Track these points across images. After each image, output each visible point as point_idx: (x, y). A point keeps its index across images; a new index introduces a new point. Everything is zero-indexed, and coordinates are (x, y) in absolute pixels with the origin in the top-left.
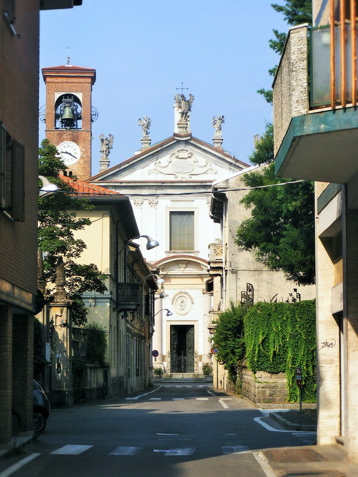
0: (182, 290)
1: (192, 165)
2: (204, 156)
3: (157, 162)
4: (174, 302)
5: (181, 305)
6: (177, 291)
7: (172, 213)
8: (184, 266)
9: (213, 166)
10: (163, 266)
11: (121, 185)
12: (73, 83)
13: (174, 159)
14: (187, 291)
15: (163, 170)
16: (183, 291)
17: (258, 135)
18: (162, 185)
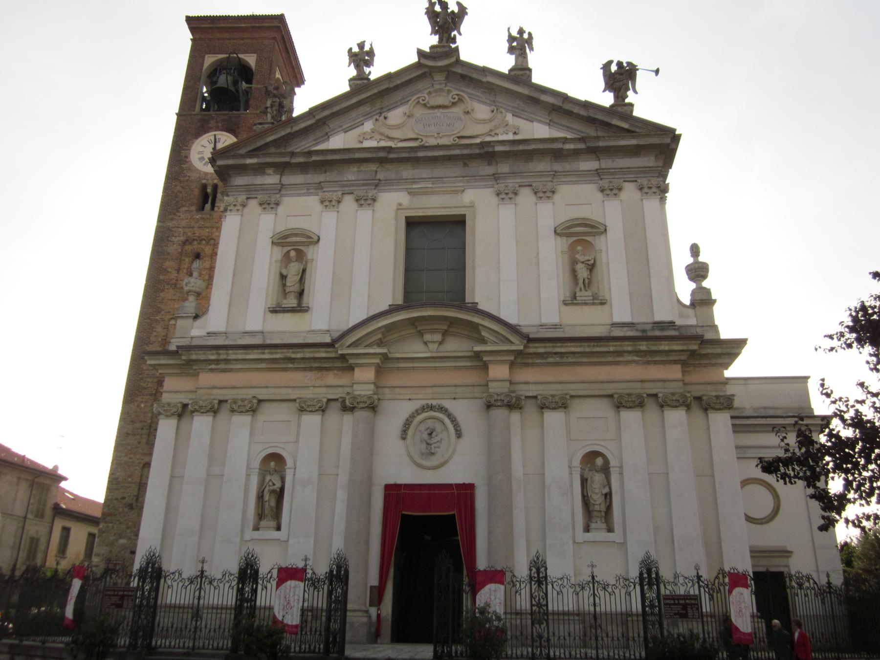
0: (430, 402)
1: (460, 119)
2: (488, 101)
3: (382, 118)
4: (410, 432)
5: (429, 441)
6: (417, 404)
7: (412, 224)
8: (438, 337)
9: (509, 117)
10: (380, 336)
11: (294, 161)
12: (243, 39)
13: (420, 112)
14: (447, 404)
15: (395, 134)
16: (434, 402)
17: (611, 62)
18: (384, 158)
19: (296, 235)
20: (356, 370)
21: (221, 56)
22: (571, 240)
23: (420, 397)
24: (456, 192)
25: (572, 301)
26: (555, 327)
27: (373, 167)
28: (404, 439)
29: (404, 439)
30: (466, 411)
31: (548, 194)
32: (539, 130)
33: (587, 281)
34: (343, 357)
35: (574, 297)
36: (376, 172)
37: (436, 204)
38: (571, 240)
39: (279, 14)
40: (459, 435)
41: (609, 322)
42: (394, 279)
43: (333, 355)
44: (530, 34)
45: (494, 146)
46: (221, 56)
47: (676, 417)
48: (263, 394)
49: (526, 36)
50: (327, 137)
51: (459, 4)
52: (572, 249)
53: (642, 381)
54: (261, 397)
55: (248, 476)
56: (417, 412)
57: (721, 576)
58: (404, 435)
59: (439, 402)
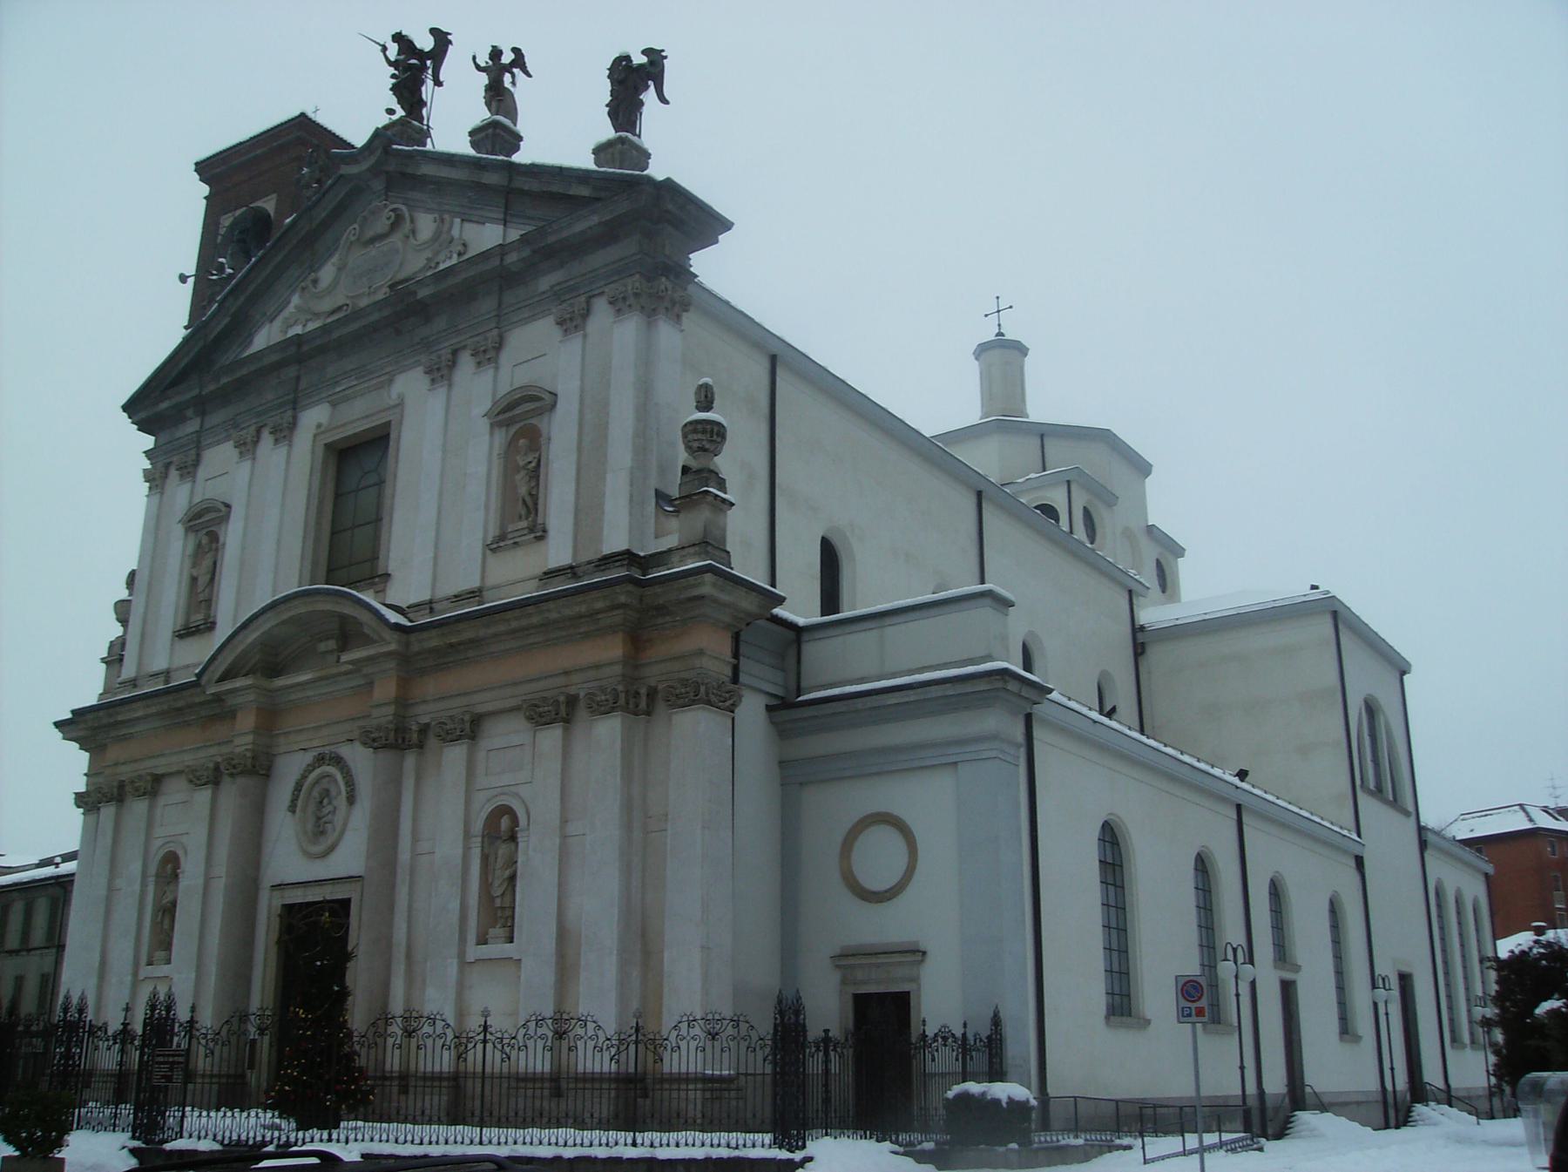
4: (299, 803)
14: (345, 751)
19: (208, 510)
20: (239, 715)
21: (238, 212)
22: (513, 430)
23: (315, 743)
24: (379, 387)
25: (498, 544)
26: (475, 594)
27: (291, 372)
28: (294, 812)
29: (294, 812)
30: (360, 758)
31: (491, 354)
32: (487, 236)
33: (528, 499)
34: (218, 698)
35: (502, 537)
36: (298, 378)
37: (356, 416)
38: (513, 430)
39: (297, 113)
40: (351, 800)
41: (539, 571)
42: (303, 558)
43: (202, 699)
44: (516, 51)
45: (415, 293)
46: (238, 212)
47: (608, 730)
48: (161, 765)
49: (507, 58)
50: (248, 341)
51: (435, 32)
52: (511, 445)
53: (566, 673)
54: (159, 771)
55: (144, 885)
56: (311, 768)
57: (235, 1021)
58: (292, 809)
59: (332, 748)
